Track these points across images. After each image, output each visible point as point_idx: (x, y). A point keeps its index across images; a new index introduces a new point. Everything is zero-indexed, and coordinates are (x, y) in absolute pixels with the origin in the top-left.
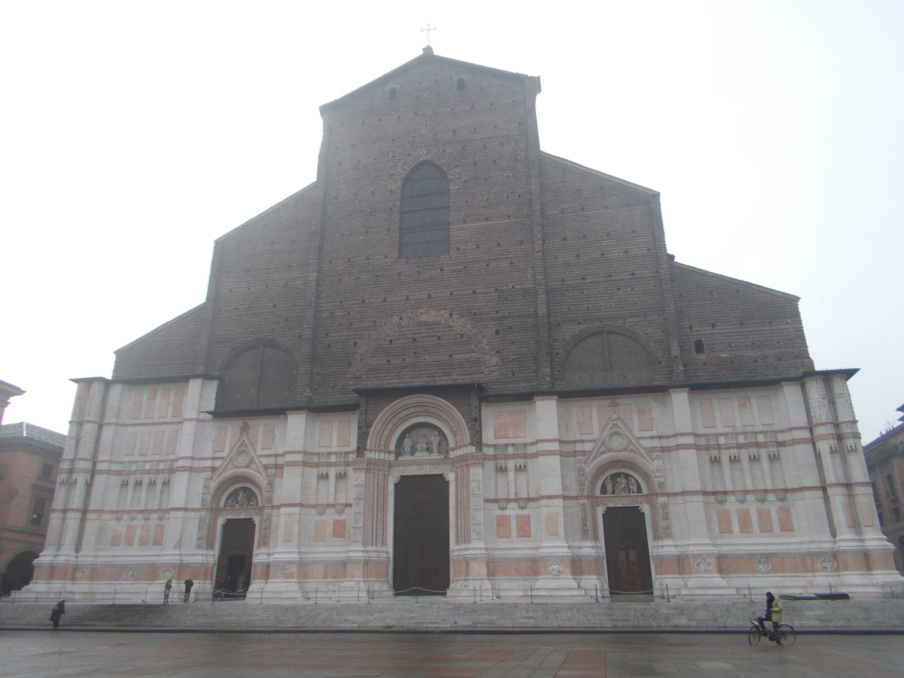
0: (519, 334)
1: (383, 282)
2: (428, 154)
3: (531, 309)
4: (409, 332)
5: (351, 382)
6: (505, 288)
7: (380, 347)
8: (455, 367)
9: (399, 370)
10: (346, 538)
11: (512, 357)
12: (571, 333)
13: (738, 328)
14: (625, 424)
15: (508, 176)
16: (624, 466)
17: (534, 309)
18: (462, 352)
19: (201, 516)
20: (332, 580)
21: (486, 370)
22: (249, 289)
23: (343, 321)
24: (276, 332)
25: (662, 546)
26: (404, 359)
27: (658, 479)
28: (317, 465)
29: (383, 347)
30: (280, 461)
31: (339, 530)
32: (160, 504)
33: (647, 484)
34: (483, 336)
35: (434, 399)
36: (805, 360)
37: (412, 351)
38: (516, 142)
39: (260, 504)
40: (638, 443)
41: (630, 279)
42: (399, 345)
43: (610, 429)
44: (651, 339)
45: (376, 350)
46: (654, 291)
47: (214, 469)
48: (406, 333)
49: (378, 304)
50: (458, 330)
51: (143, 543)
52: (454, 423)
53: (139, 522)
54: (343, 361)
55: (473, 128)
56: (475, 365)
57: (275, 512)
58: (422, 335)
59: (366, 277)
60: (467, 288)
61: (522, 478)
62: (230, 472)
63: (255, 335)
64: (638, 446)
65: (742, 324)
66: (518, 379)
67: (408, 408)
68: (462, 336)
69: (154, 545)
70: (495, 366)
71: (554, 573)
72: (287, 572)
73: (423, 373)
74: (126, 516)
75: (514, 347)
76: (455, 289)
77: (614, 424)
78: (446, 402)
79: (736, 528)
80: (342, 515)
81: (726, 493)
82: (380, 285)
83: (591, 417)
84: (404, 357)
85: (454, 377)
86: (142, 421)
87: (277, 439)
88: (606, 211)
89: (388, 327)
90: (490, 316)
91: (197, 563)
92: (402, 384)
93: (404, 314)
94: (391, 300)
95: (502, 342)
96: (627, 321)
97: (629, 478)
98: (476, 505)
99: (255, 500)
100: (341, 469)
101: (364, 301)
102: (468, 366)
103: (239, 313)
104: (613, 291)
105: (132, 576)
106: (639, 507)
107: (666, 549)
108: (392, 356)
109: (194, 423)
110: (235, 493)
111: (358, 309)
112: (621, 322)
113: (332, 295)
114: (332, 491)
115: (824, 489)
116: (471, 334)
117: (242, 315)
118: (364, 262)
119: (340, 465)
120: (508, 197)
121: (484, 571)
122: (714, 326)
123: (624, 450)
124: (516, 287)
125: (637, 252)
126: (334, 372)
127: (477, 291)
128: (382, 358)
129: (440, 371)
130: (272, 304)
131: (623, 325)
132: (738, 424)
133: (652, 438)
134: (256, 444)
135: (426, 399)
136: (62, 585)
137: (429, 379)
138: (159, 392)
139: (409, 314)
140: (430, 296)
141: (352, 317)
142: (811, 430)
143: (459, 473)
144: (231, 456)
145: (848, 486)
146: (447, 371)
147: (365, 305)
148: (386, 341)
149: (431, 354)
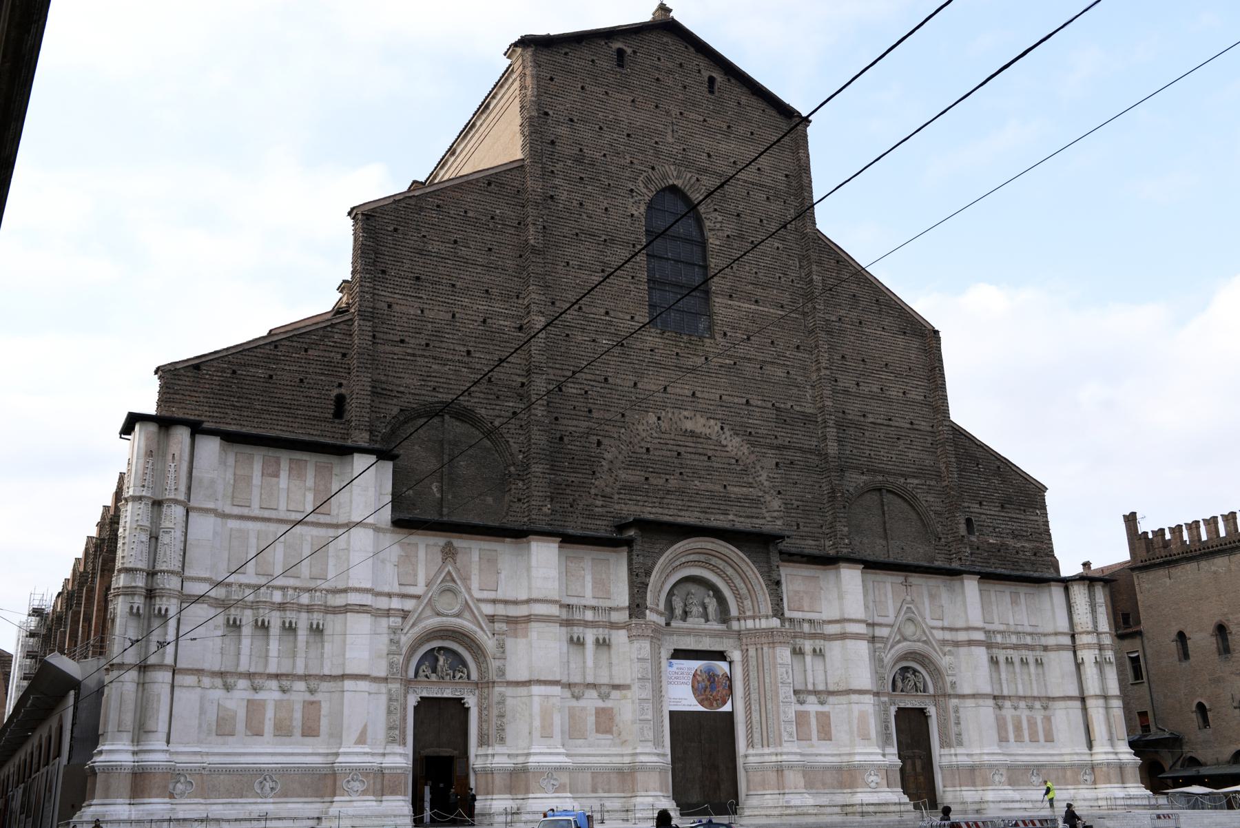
0: (801, 474)
1: (632, 357)
2: (678, 177)
3: (812, 443)
4: (672, 442)
5: (597, 502)
6: (782, 406)
7: (635, 455)
8: (732, 503)
9: (662, 496)
10: (615, 735)
11: (796, 503)
12: (855, 485)
13: (999, 511)
14: (917, 608)
15: (778, 248)
16: (914, 660)
17: (816, 444)
18: (739, 484)
19: (390, 690)
20: (606, 795)
21: (767, 515)
22: (422, 311)
23: (577, 404)
24: (430, 386)
25: (956, 755)
26: (667, 480)
27: (951, 678)
28: (568, 623)
29: (638, 456)
30: (513, 611)
31: (605, 722)
32: (306, 666)
33: (935, 686)
34: (762, 468)
35: (724, 547)
36: (1053, 559)
37: (678, 471)
38: (785, 202)
39: (474, 676)
40: (931, 633)
41: (910, 429)
42: (660, 459)
43: (905, 613)
44: (932, 508)
45: (629, 459)
46: (931, 450)
47: (405, 614)
48: (668, 442)
49: (626, 389)
50: (733, 453)
51: (283, 730)
52: (745, 583)
53: (271, 694)
54: (585, 467)
55: (732, 160)
56: (755, 506)
57: (510, 691)
58: (689, 450)
59: (607, 342)
60: (739, 394)
61: (819, 664)
62: (433, 622)
63: (440, 395)
64: (931, 638)
65: (1002, 507)
66: (804, 534)
67: (687, 555)
68: (737, 461)
69: (303, 735)
70: (778, 511)
71: (873, 785)
72: (555, 783)
73: (693, 504)
74: (243, 683)
75: (796, 489)
76: (725, 393)
77: (907, 608)
78: (741, 554)
79: (1011, 736)
80: (607, 701)
81: (1004, 697)
82: (627, 361)
83: (886, 595)
84: (668, 477)
85: (731, 517)
86: (256, 512)
87: (502, 576)
88: (883, 333)
89: (643, 427)
90: (768, 441)
91: (396, 768)
92: (668, 517)
93: (664, 413)
94: (644, 387)
95: (784, 480)
96: (908, 481)
97: (917, 674)
98: (786, 697)
99: (465, 670)
100: (602, 633)
101: (606, 380)
102: (747, 505)
103: (409, 351)
104: (894, 440)
105: (272, 789)
106: (926, 708)
107: (959, 758)
108: (652, 472)
109: (371, 532)
110: (431, 656)
111: (599, 389)
112: (902, 480)
113: (559, 358)
114: (590, 662)
115: (1083, 700)
116: (748, 461)
117: (414, 355)
118: (602, 317)
119: (604, 627)
120: (780, 278)
121: (801, 782)
122: (981, 504)
123: (919, 641)
124: (794, 407)
125: (914, 397)
126: (573, 482)
127: (751, 402)
128: (638, 473)
129: (713, 506)
130: (465, 349)
131: (905, 485)
132: (1011, 622)
133: (943, 629)
134: (470, 579)
135: (714, 545)
136: (169, 806)
137: (702, 516)
138: (285, 465)
139: (670, 415)
140: (694, 394)
141: (592, 401)
142: (1073, 636)
143: (752, 652)
144: (430, 595)
145: (1106, 697)
146: (722, 507)
147: (609, 386)
148: (642, 448)
149: (702, 480)
